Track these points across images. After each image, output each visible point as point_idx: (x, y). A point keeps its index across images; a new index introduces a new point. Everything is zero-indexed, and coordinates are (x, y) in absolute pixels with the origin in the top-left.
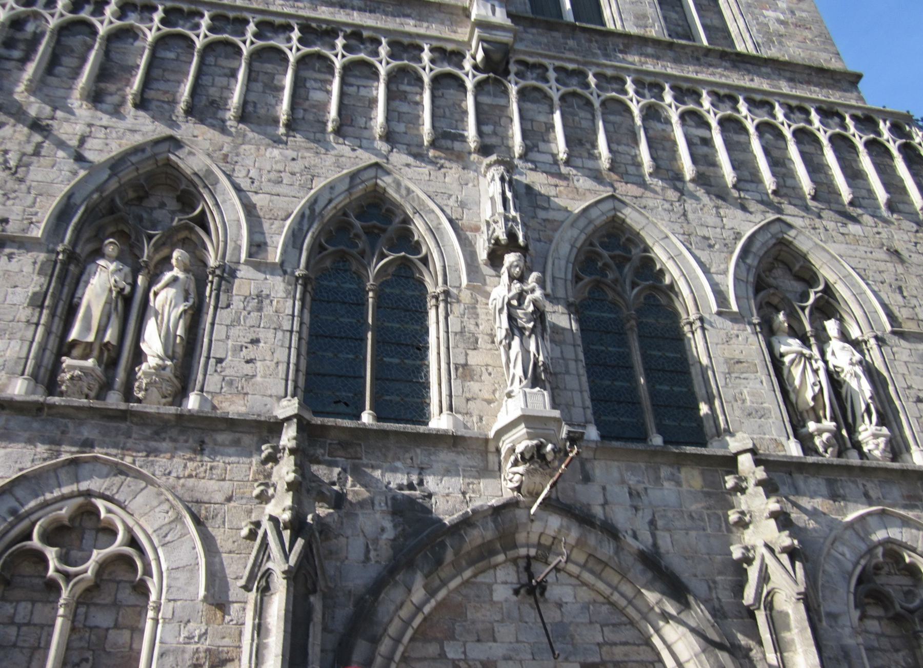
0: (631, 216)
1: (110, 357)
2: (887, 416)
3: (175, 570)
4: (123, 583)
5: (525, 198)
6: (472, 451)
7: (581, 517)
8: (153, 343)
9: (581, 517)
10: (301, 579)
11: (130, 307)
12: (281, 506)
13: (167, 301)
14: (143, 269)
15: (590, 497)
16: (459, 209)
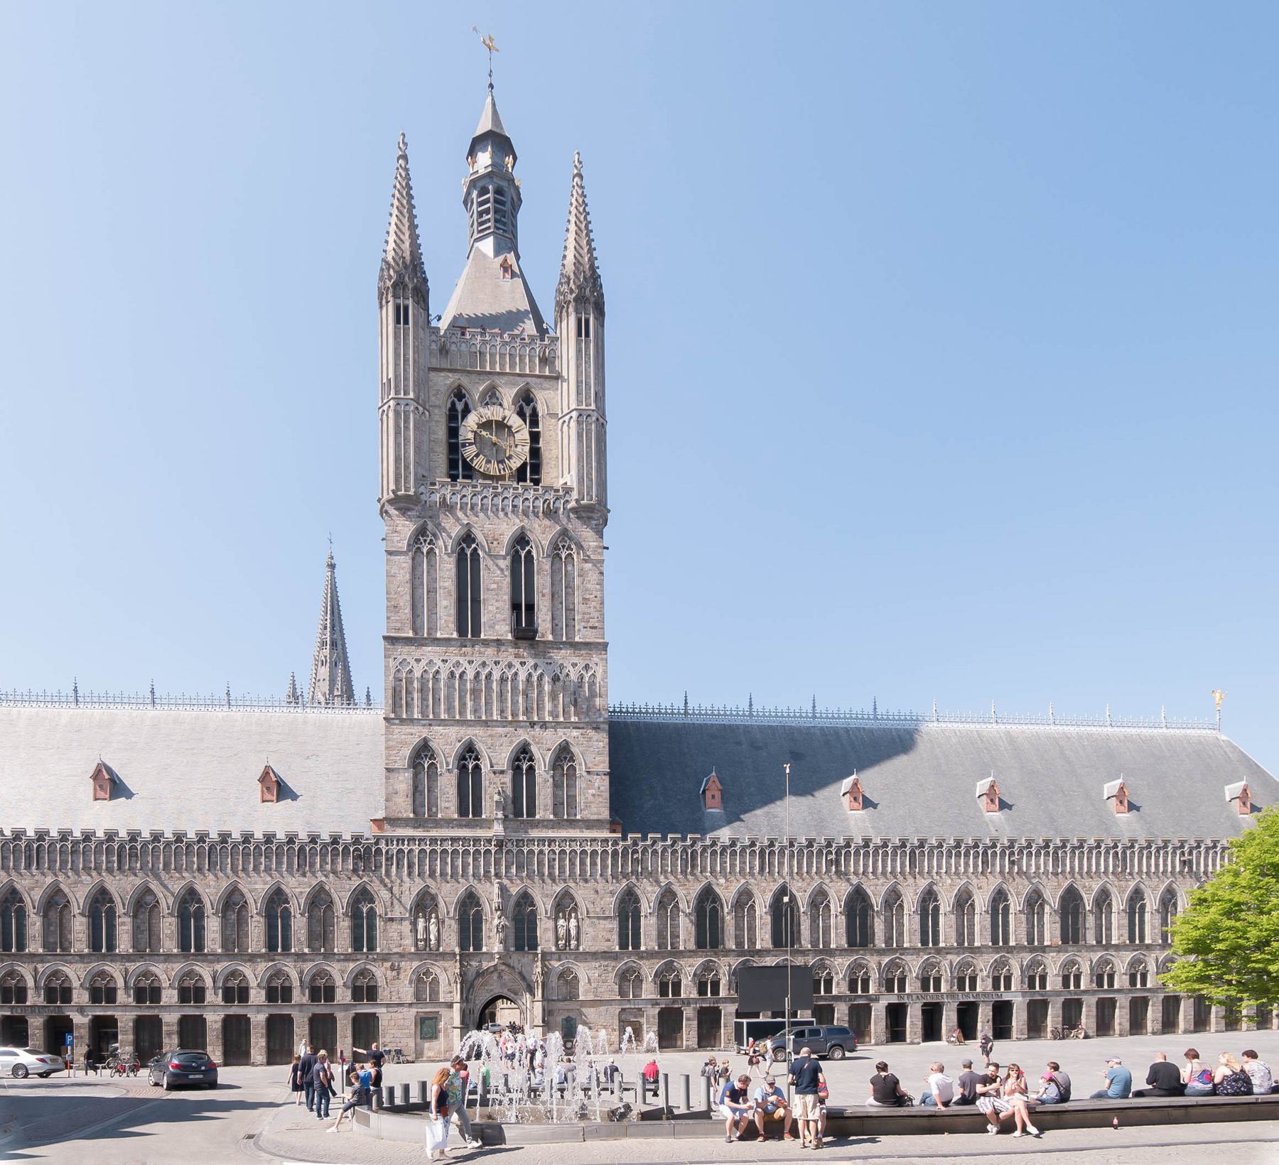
0: (530, 891)
1: (425, 940)
2: (578, 939)
3: (443, 979)
4: (435, 981)
5: (503, 889)
6: (490, 955)
7: (509, 966)
8: (432, 937)
9: (509, 966)
10: (462, 983)
11: (426, 929)
12: (458, 971)
13: (433, 928)
14: (428, 920)
15: (511, 962)
16: (490, 894)
